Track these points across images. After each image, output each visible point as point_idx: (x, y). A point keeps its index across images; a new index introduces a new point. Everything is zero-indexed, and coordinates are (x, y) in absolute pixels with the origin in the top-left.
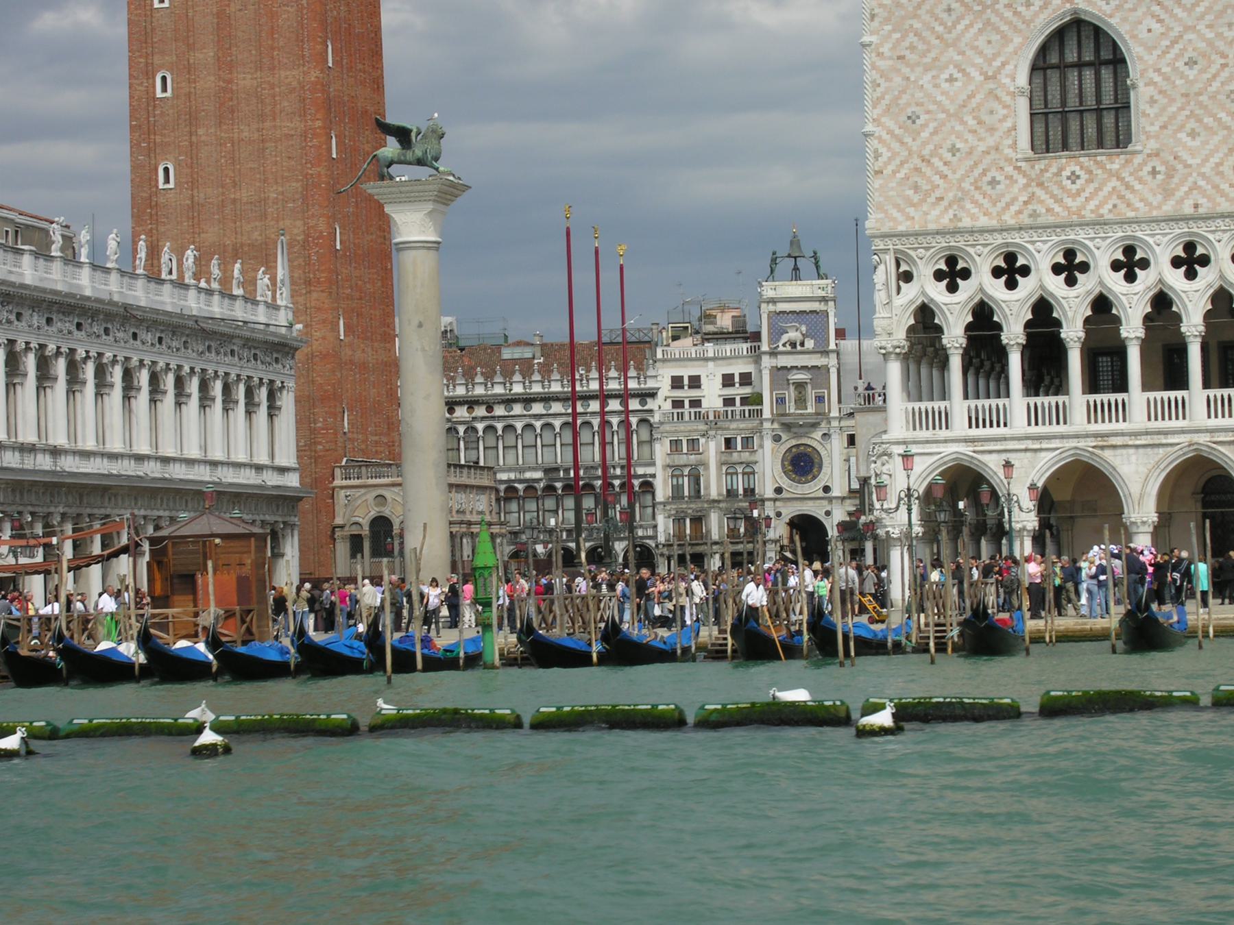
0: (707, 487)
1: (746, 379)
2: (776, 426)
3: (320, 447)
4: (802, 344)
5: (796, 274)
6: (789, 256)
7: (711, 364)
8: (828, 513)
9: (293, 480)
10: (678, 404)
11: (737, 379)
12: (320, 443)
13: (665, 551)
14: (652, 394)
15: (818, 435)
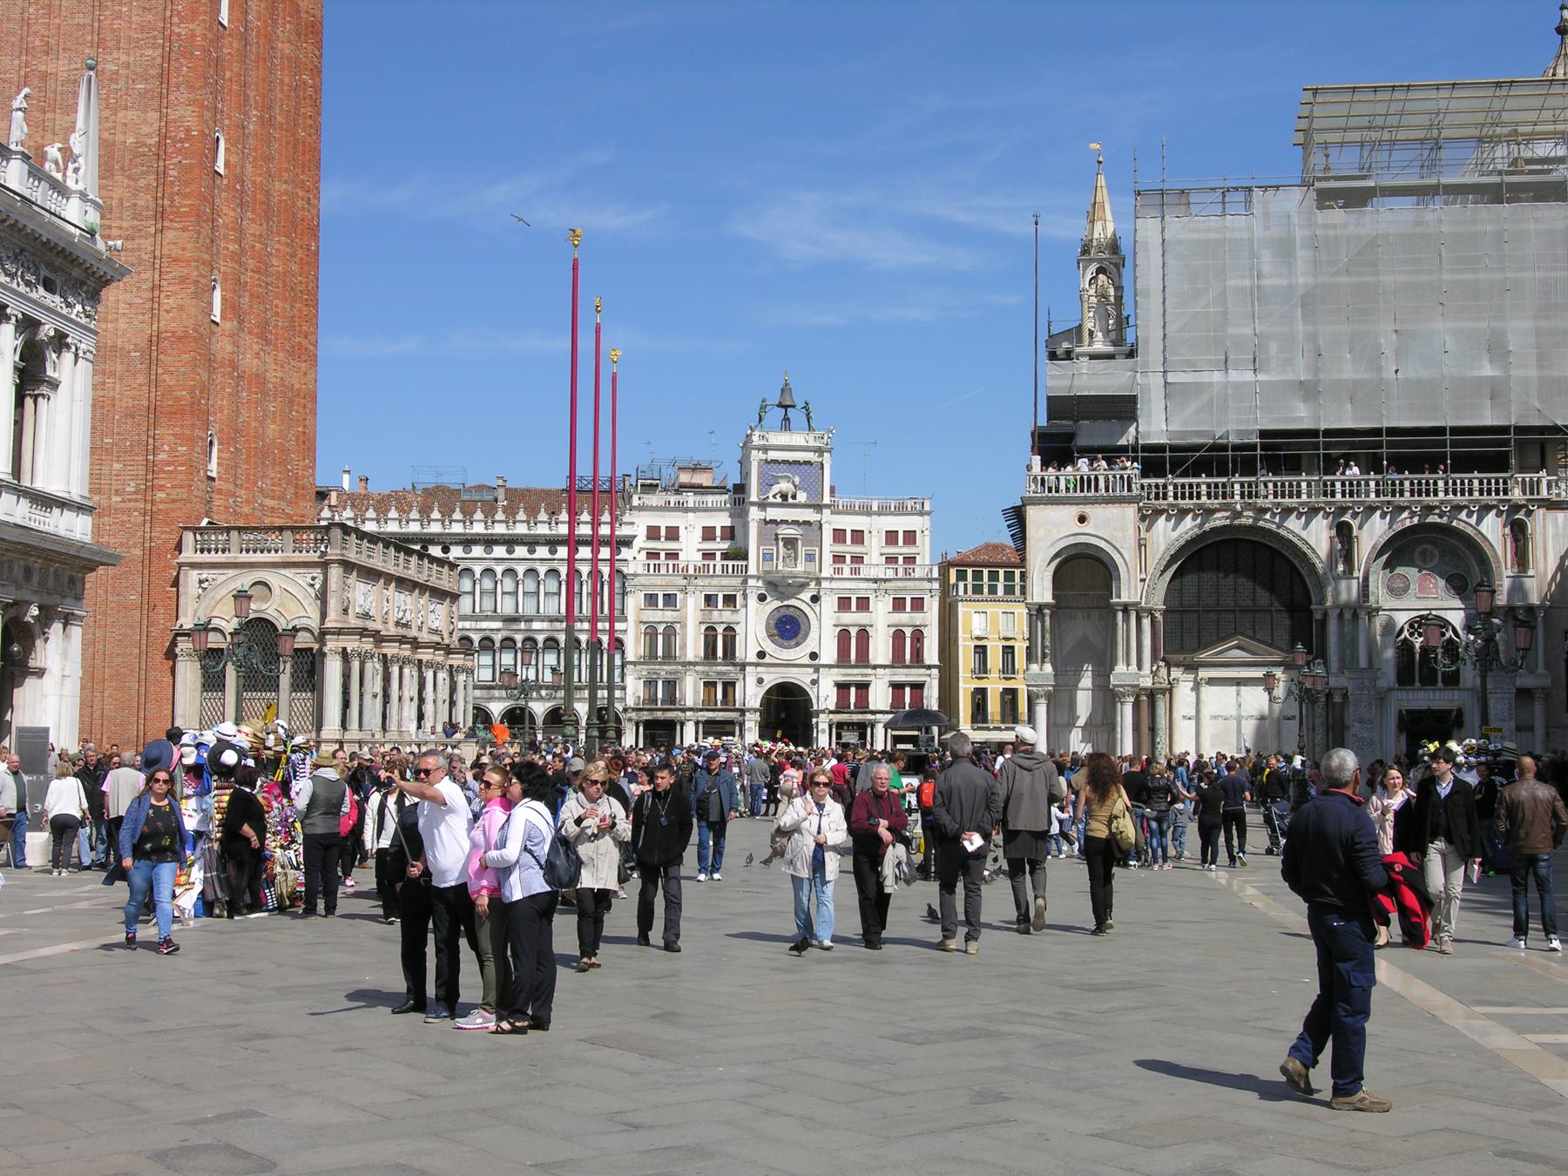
0: (684, 646)
1: (729, 533)
2: (760, 584)
3: (161, 495)
4: (794, 497)
5: (786, 424)
6: (780, 405)
7: (691, 515)
8: (814, 682)
9: (74, 528)
10: (653, 555)
11: (718, 533)
12: (162, 488)
13: (633, 715)
14: (627, 542)
15: (806, 595)
